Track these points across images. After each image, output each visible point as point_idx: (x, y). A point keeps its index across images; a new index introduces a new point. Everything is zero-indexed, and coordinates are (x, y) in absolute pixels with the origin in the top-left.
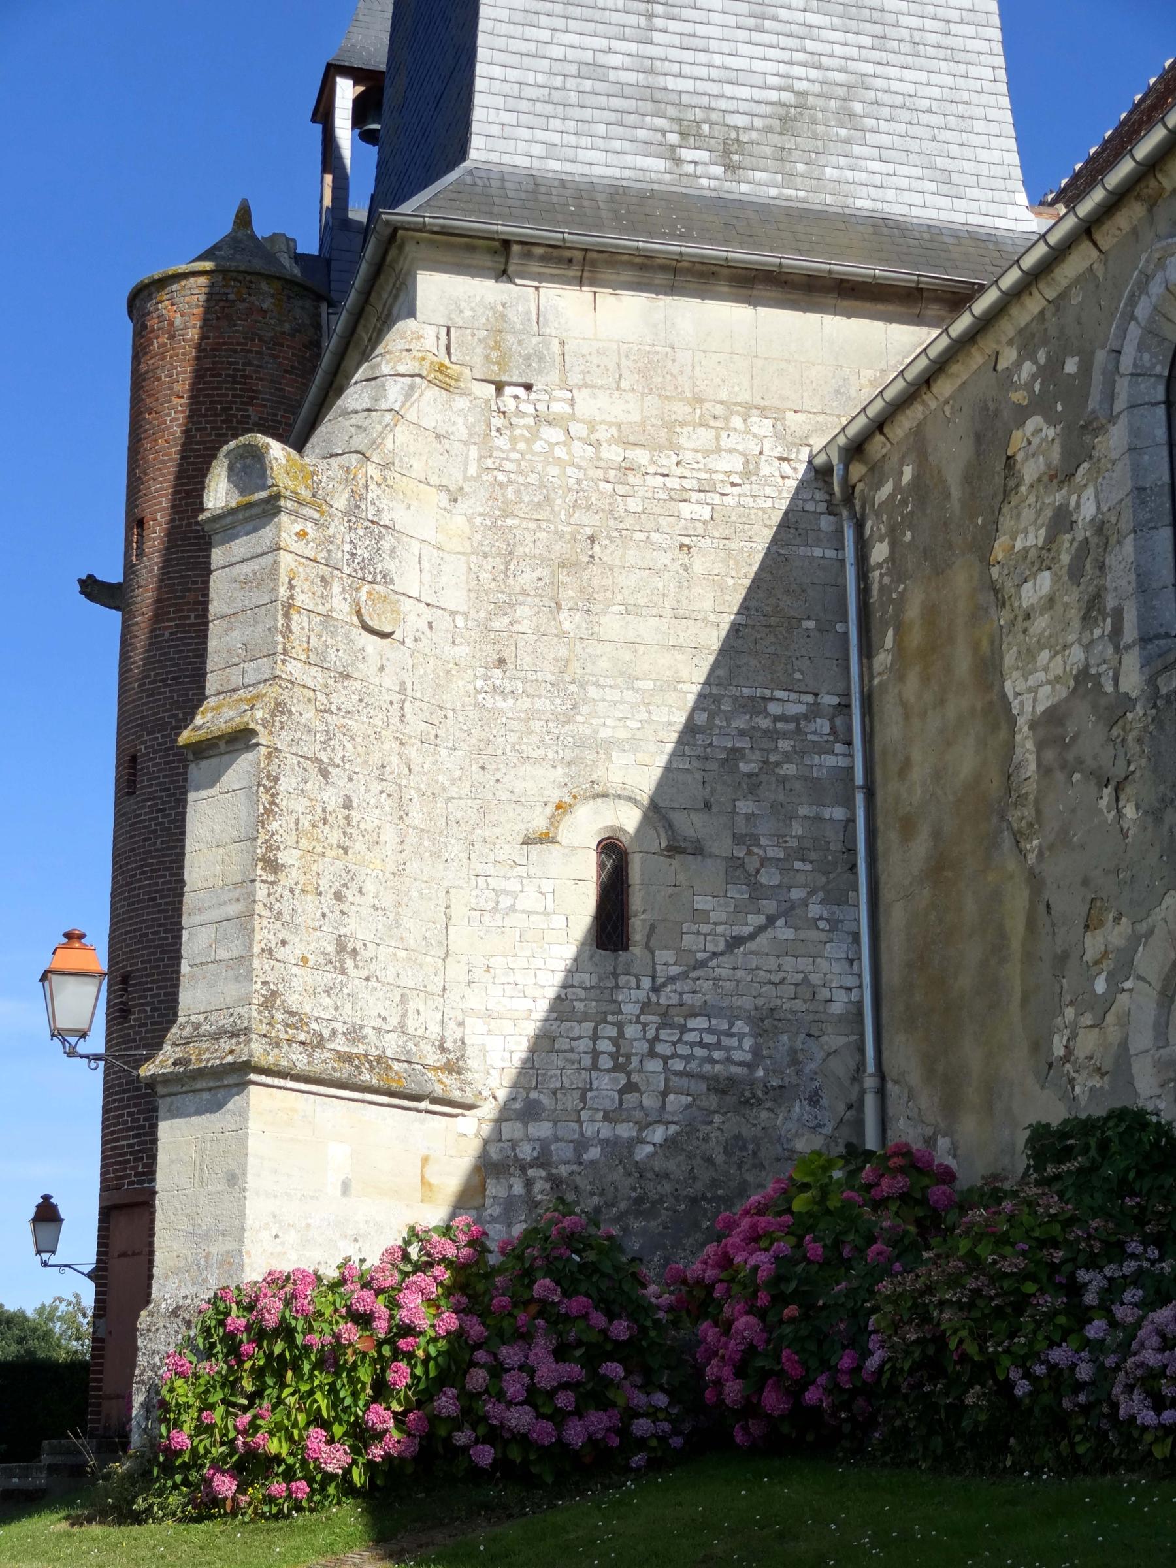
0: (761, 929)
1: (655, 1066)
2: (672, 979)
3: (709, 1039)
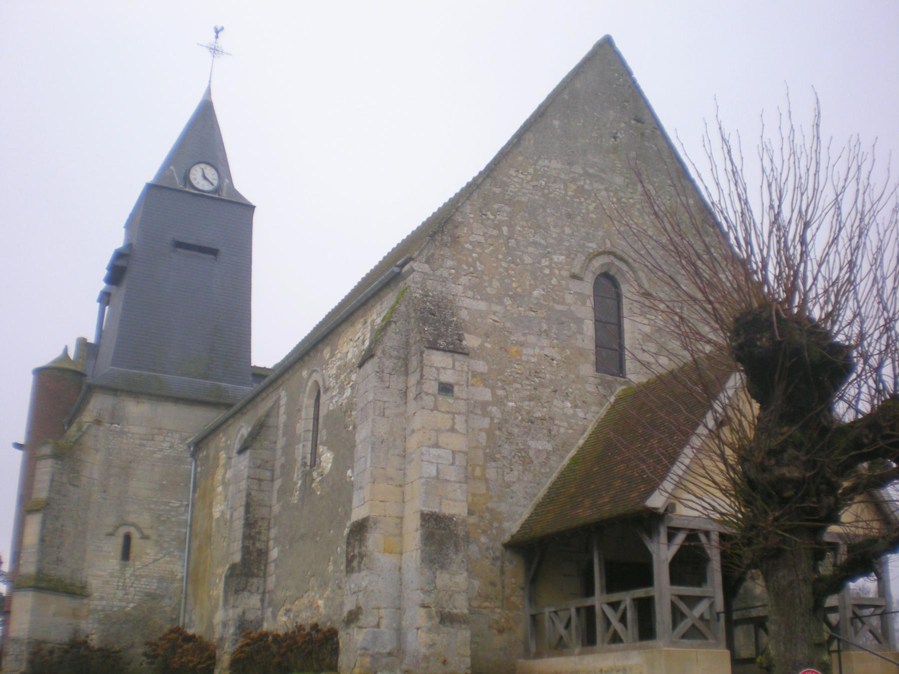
1: (132, 589)
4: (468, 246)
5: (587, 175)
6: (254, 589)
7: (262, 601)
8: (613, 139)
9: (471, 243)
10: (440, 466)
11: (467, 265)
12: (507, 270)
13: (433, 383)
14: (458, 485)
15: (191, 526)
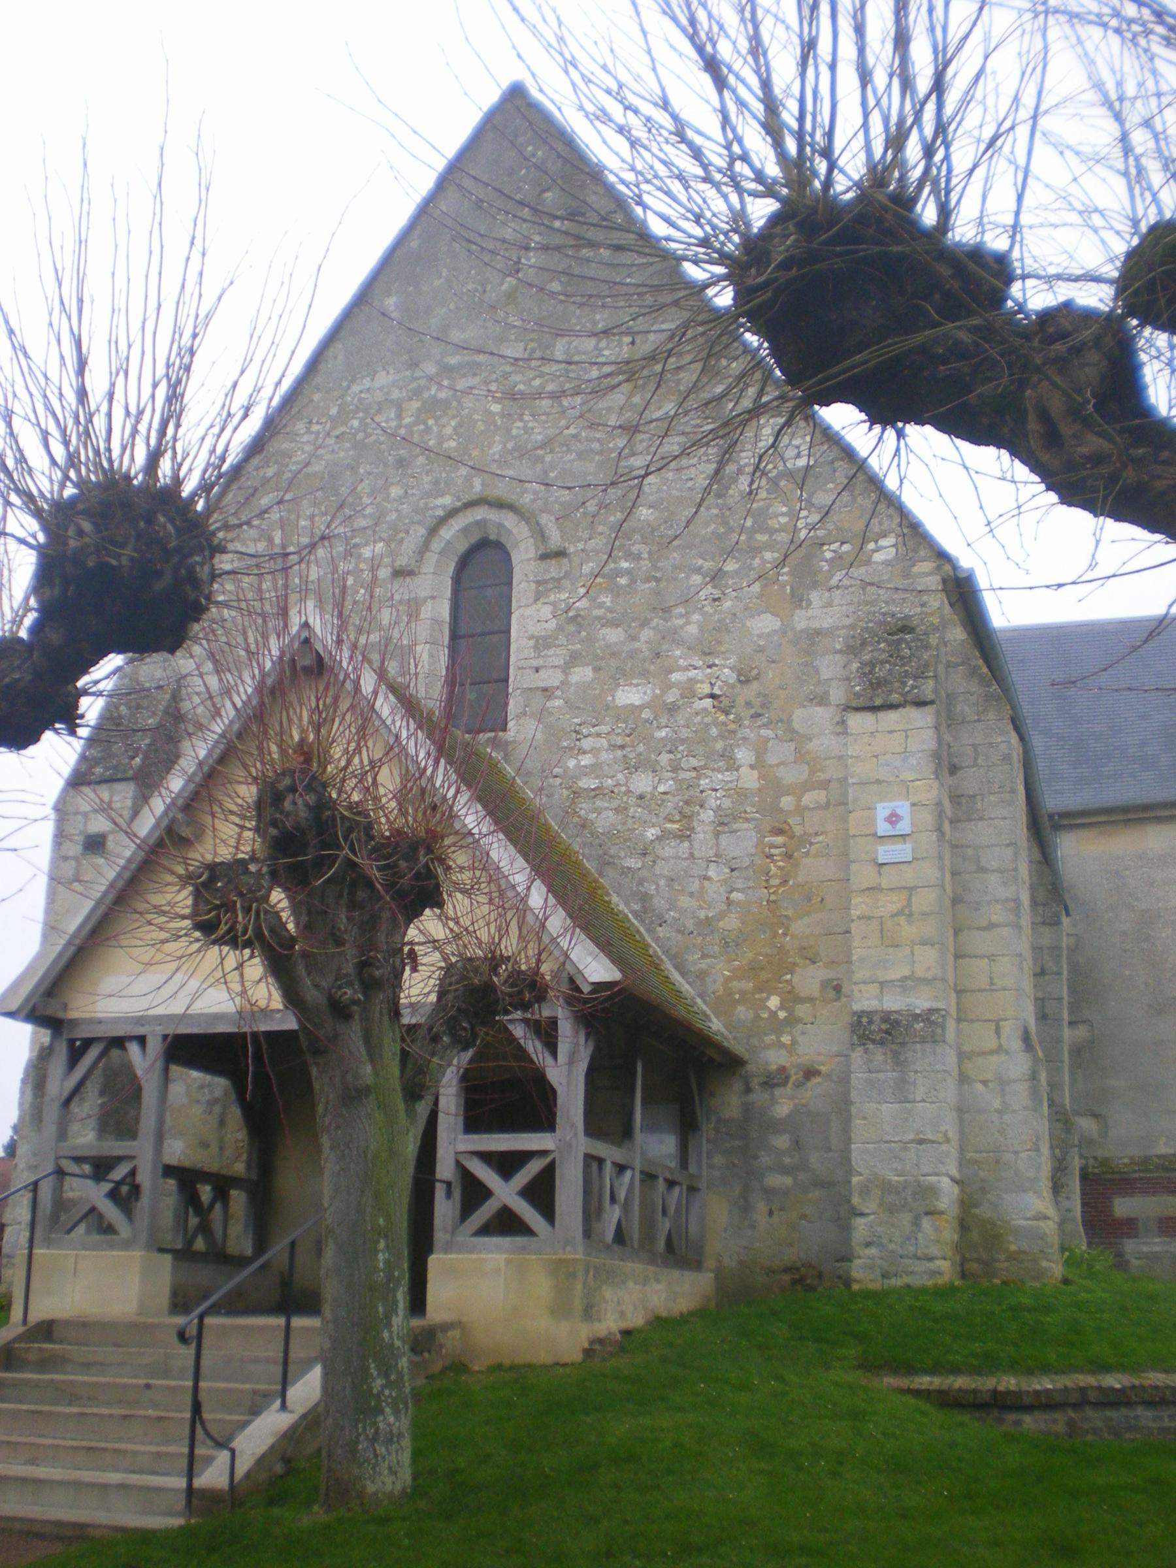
5: (447, 370)
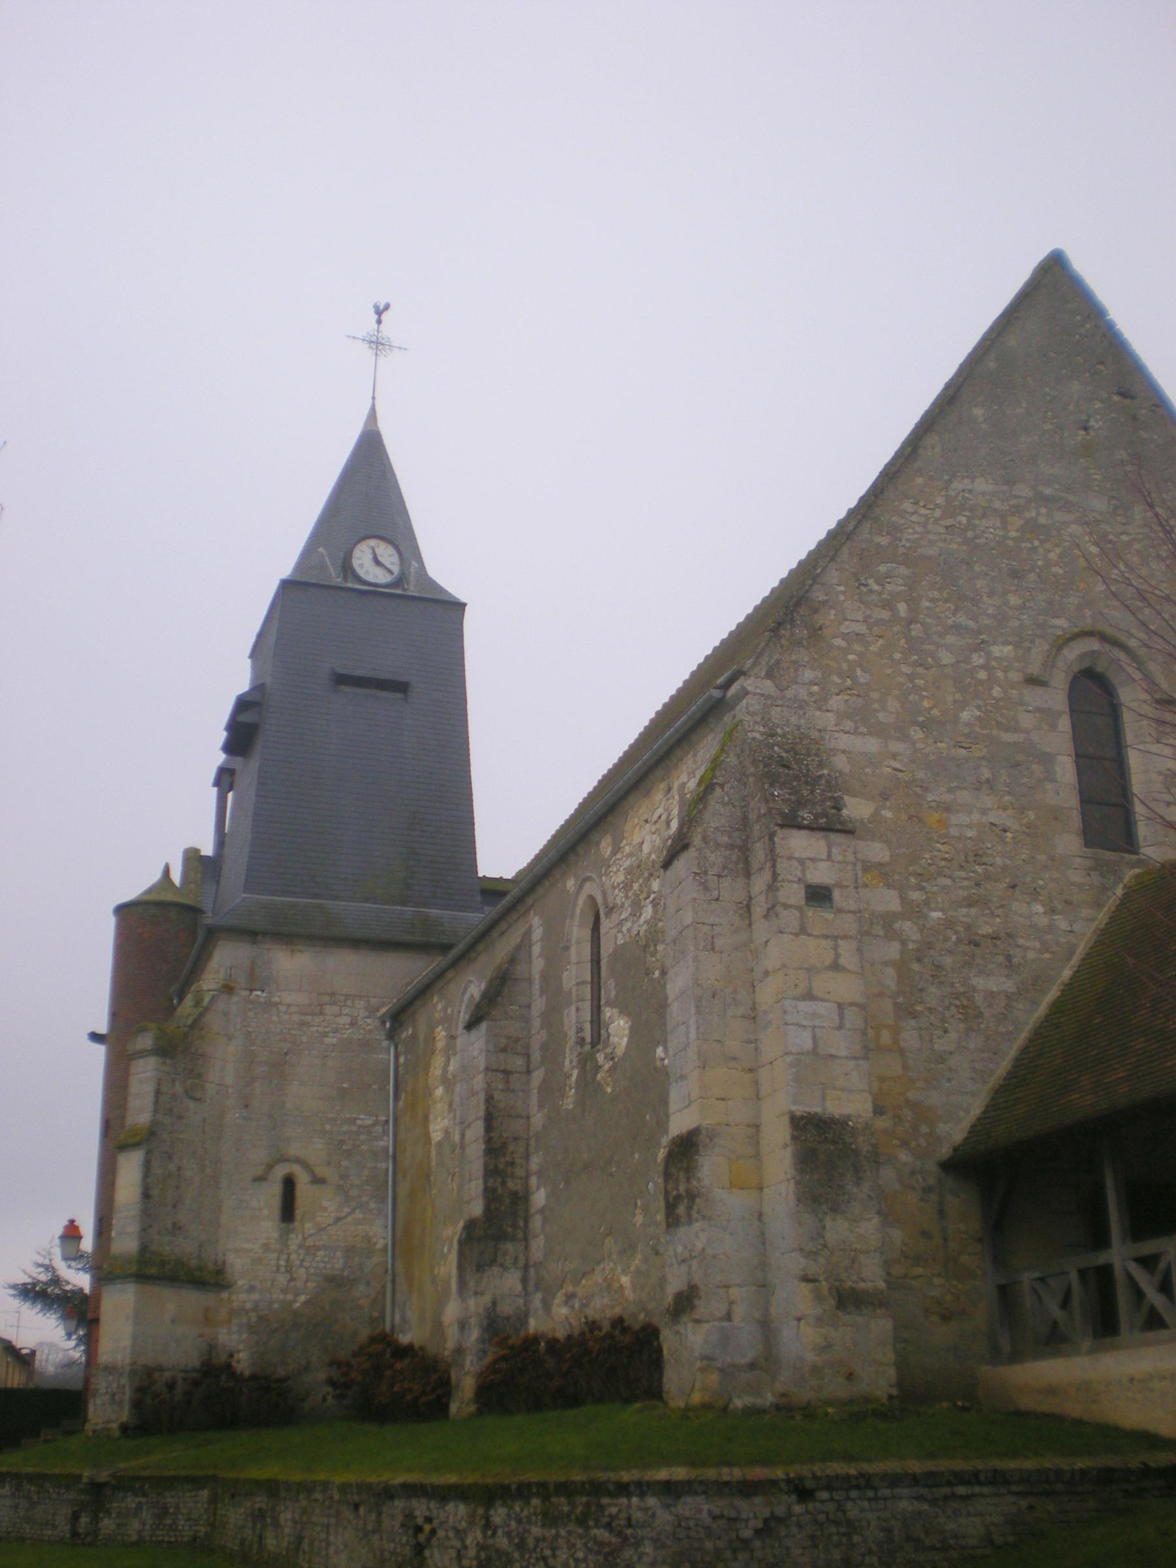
0: (349, 1214)
1: (302, 1271)
2: (311, 1235)
3: (326, 1259)
4: (839, 642)
6: (509, 1261)
7: (524, 1281)
8: (1082, 432)
9: (845, 636)
10: (817, 1030)
11: (840, 676)
12: (911, 677)
13: (795, 886)
14: (852, 1063)
15: (394, 1158)
